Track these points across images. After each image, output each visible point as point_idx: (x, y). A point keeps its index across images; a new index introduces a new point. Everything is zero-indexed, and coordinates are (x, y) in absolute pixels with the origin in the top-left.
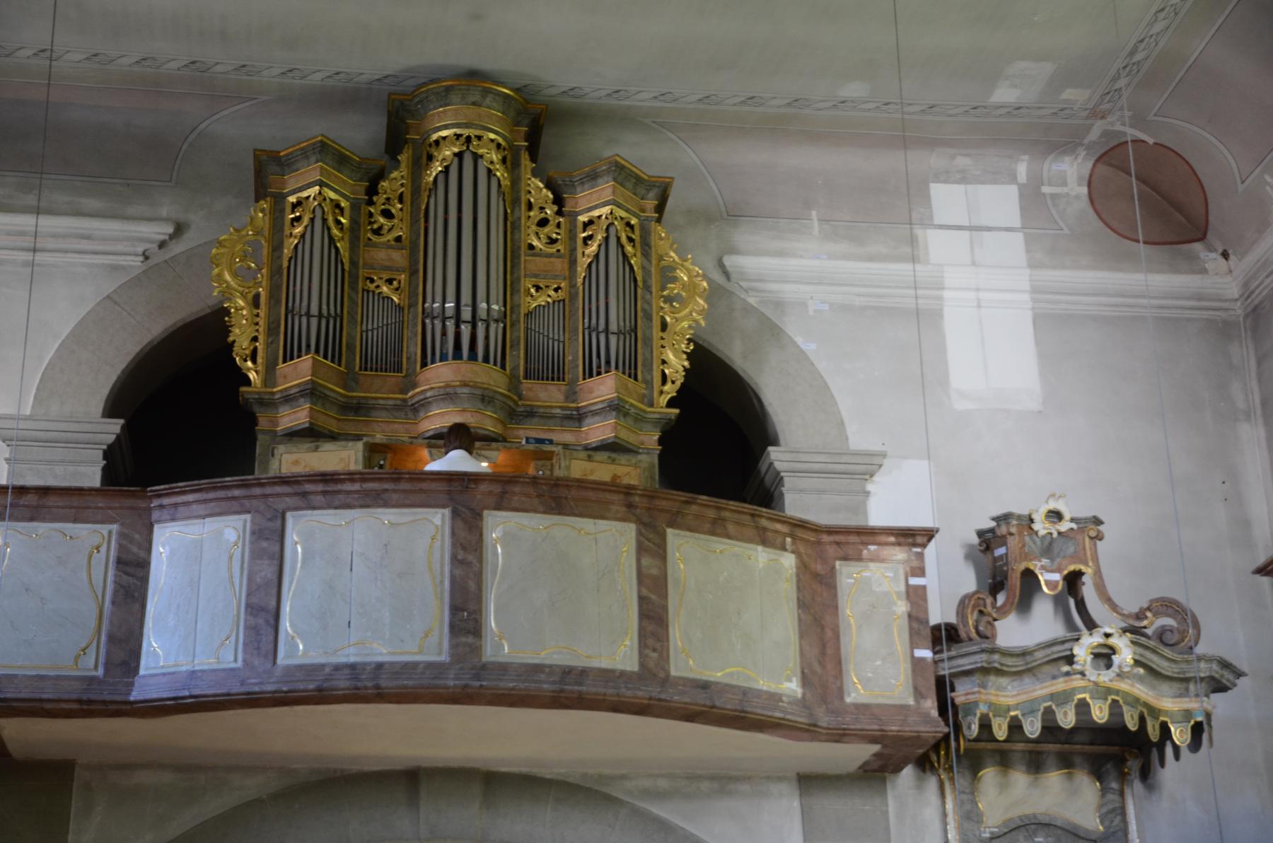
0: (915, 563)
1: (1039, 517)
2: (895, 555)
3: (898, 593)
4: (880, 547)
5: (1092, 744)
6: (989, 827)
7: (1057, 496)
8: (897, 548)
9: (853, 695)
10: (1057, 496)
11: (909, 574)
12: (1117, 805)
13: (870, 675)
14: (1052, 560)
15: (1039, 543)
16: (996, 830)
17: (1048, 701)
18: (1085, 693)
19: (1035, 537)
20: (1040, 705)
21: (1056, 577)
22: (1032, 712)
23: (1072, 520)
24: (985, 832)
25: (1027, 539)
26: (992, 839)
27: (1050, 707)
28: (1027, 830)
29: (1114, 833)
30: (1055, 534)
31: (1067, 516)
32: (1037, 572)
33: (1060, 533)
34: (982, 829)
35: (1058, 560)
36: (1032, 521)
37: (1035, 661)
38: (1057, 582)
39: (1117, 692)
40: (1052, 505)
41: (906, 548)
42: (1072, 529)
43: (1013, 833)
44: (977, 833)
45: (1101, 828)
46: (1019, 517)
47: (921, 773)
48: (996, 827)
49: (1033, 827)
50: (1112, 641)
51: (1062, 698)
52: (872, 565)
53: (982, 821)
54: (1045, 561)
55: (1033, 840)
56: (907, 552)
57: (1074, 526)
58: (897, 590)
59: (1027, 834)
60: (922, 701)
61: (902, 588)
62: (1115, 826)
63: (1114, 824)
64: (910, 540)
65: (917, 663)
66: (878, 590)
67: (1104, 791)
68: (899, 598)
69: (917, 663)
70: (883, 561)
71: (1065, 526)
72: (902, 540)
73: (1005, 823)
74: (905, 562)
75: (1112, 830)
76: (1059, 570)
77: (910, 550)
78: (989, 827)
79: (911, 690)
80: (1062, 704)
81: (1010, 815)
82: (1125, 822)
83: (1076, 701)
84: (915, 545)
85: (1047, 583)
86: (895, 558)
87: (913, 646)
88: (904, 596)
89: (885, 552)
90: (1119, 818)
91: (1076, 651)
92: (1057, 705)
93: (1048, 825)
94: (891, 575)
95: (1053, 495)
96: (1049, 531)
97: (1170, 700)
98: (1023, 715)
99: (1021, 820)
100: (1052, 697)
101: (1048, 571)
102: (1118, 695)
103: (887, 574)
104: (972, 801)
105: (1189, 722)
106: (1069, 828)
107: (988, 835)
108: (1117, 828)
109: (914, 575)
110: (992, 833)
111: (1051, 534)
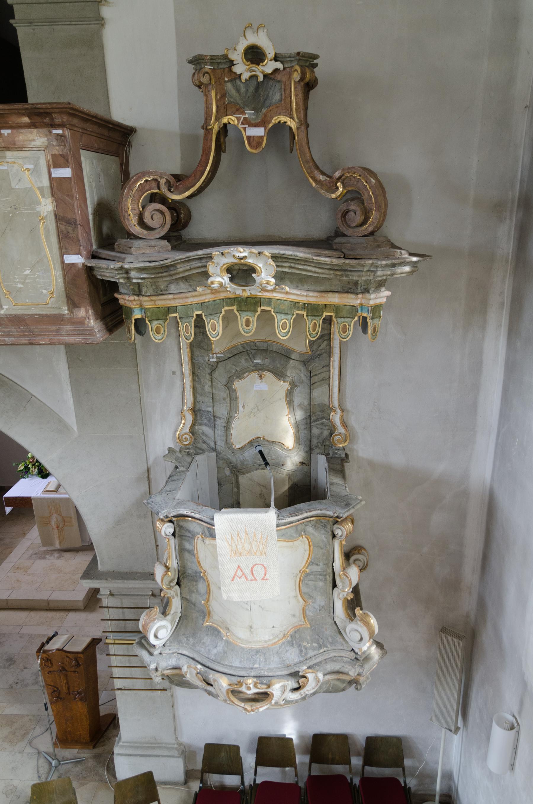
0: (57, 150)
1: (237, 56)
2: (34, 140)
3: (41, 189)
4: (15, 131)
6: (216, 354)
7: (255, 26)
8: (35, 131)
9: (5, 307)
10: (255, 26)
11: (52, 166)
13: (20, 285)
14: (257, 110)
15: (243, 90)
16: (222, 355)
17: (200, 310)
19: (238, 81)
20: (193, 312)
21: (260, 132)
22: (188, 317)
23: (276, 59)
24: (213, 358)
25: (229, 86)
26: (217, 362)
27: (202, 314)
28: (248, 354)
29: (320, 355)
30: (261, 78)
31: (270, 53)
32: (240, 126)
33: (265, 76)
34: (211, 355)
35: (264, 111)
36: (231, 63)
37: (178, 273)
38: (262, 137)
39: (269, 301)
40: (252, 39)
41: (45, 130)
42: (276, 70)
43: (237, 357)
44: (207, 359)
45: (309, 351)
46: (213, 59)
48: (222, 353)
49: (253, 351)
50: (250, 261)
52: (9, 154)
53: (211, 350)
54: (249, 113)
55: (253, 362)
56: (46, 135)
57: (279, 65)
58: (41, 185)
59: (248, 357)
60: (76, 311)
61: (46, 183)
62: (322, 350)
63: (321, 348)
64: (47, 120)
65: (67, 268)
66: (17, 187)
68: (43, 196)
69: (67, 268)
70: (20, 148)
71: (269, 66)
72: (38, 119)
73: (229, 350)
74: (46, 148)
75: (318, 353)
76: (262, 124)
77: (50, 132)
78: (216, 354)
79: (64, 299)
80: (211, 314)
81: (234, 343)
82: (329, 345)
83: (223, 313)
84: (54, 126)
85: (249, 138)
86: (33, 144)
87: (63, 250)
88: (48, 192)
89: (21, 137)
90: (325, 343)
91: (211, 269)
93: (266, 350)
94: (31, 167)
95: (250, 26)
96: (254, 73)
97: (336, 295)
98: (180, 318)
99: (244, 348)
101: (252, 125)
102: (269, 305)
103: (26, 167)
104: (203, 333)
106: (283, 352)
107: (215, 360)
108: (323, 351)
109: (57, 166)
110: (217, 358)
111: (256, 77)
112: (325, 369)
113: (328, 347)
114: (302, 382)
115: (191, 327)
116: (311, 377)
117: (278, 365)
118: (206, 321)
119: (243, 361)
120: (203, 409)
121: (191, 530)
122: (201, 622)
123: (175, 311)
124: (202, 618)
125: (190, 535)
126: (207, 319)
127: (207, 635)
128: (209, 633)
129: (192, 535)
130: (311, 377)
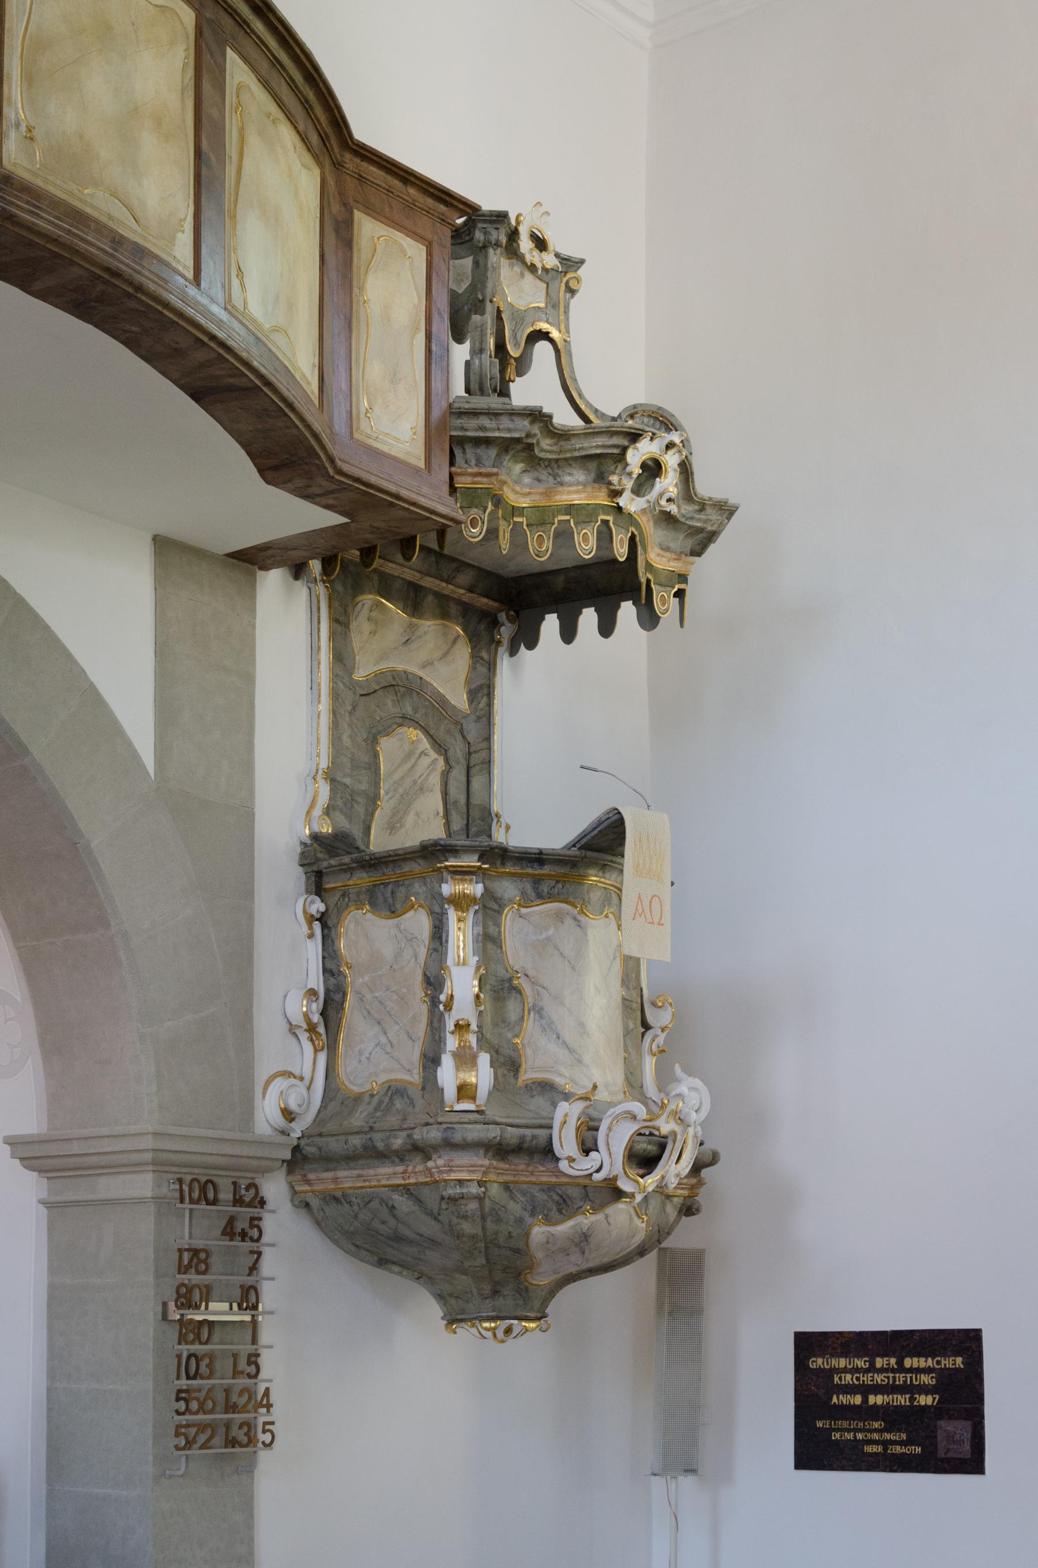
5: (471, 590)
12: (483, 682)
18: (608, 514)
20: (554, 516)
27: (569, 521)
47: (291, 580)
49: (402, 689)
51: (581, 513)
67: (475, 657)
92: (575, 524)
98: (527, 526)
99: (394, 678)
100: (570, 509)
105: (674, 587)
112: (485, 745)
113: (487, 708)
114: (458, 763)
115: (549, 539)
116: (470, 753)
117: (431, 723)
118: (575, 530)
119: (389, 703)
120: (338, 779)
121: (499, 895)
122: (512, 1081)
123: (522, 515)
124: (512, 1074)
125: (496, 907)
126: (576, 527)
127: (533, 1096)
128: (535, 1092)
129: (500, 906)
130: (470, 753)
